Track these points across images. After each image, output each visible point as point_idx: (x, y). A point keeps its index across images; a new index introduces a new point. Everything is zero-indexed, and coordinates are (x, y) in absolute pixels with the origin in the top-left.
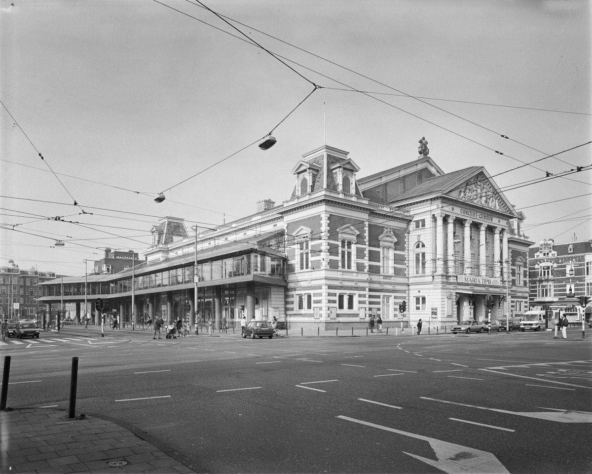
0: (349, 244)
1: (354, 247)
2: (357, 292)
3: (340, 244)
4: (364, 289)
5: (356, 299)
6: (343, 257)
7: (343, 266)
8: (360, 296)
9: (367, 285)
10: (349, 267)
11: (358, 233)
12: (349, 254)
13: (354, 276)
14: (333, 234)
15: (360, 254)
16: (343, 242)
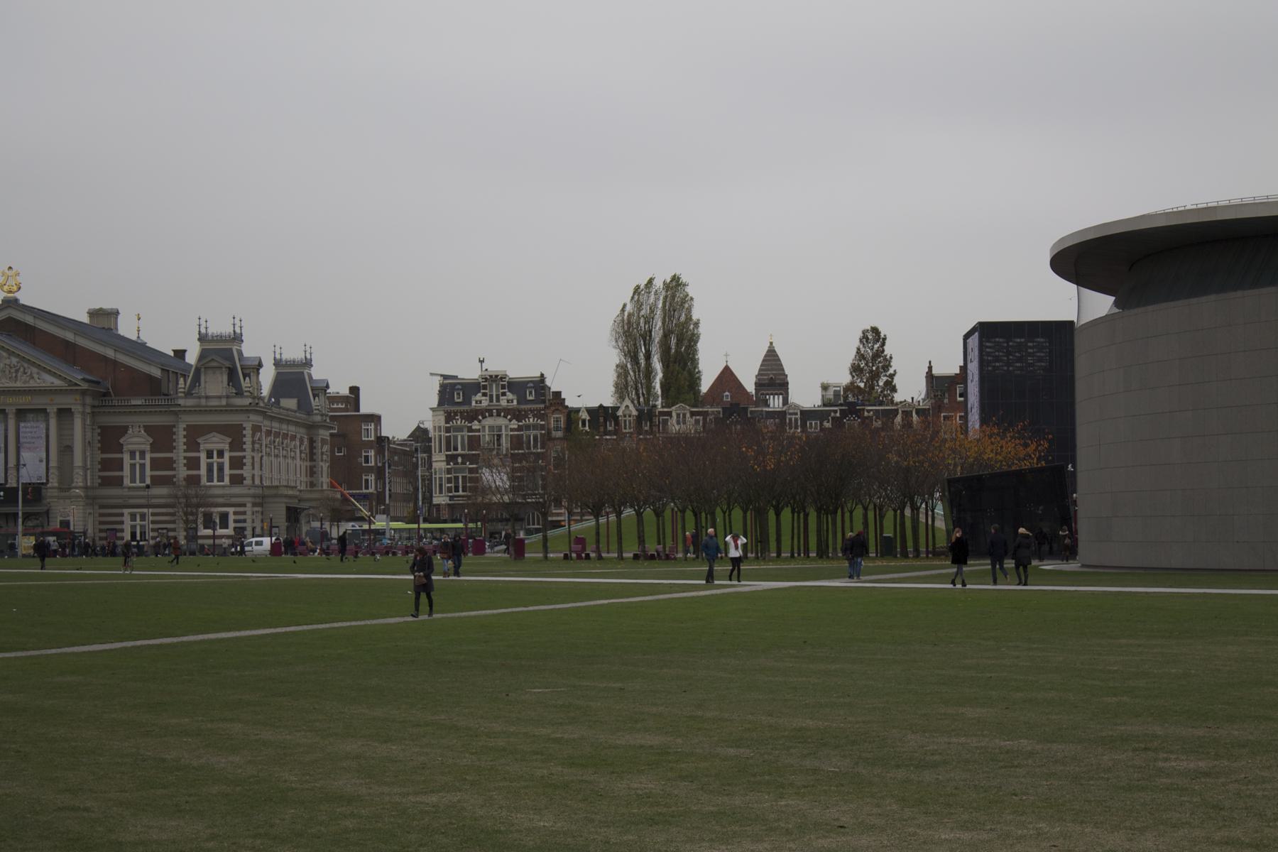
0: (221, 454)
1: (227, 455)
2: (231, 510)
3: (203, 456)
4: (244, 505)
5: (231, 518)
6: (210, 469)
7: (210, 479)
8: (235, 513)
9: (249, 499)
10: (221, 479)
11: (229, 440)
12: (221, 469)
13: (227, 491)
14: (193, 445)
15: (237, 463)
16: (210, 455)
